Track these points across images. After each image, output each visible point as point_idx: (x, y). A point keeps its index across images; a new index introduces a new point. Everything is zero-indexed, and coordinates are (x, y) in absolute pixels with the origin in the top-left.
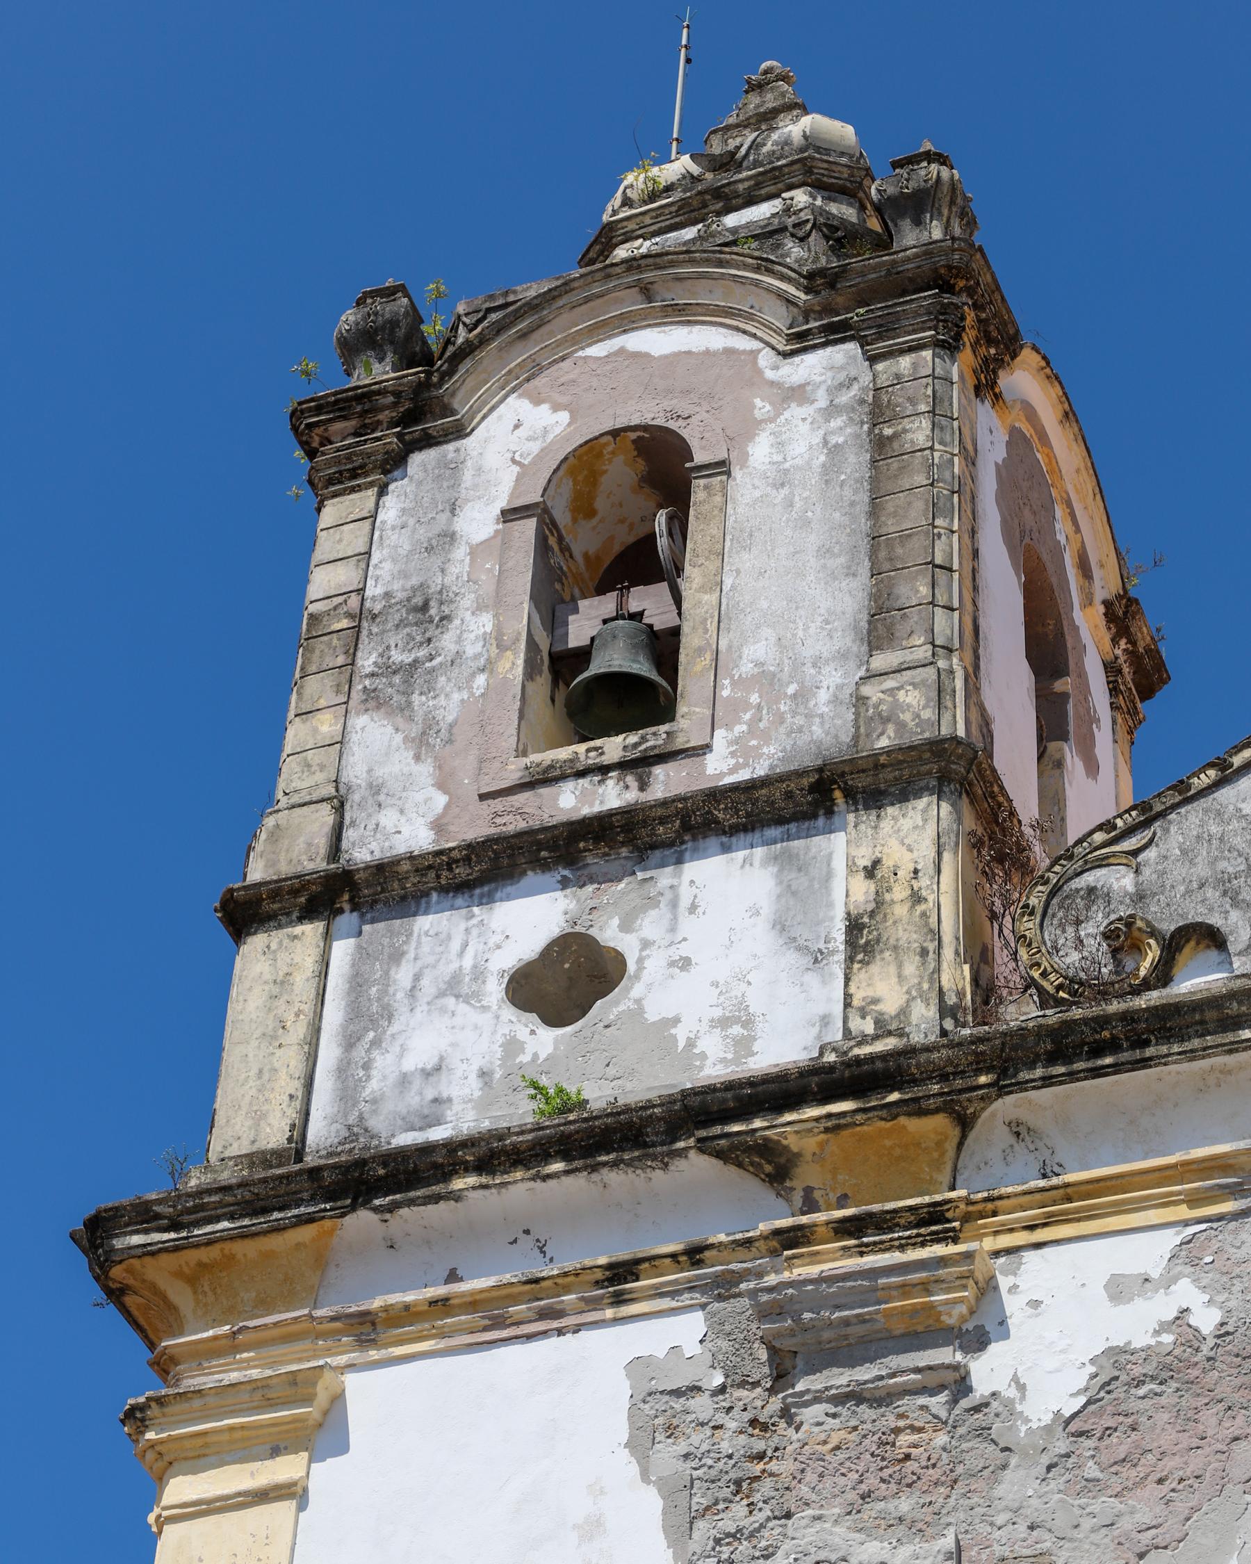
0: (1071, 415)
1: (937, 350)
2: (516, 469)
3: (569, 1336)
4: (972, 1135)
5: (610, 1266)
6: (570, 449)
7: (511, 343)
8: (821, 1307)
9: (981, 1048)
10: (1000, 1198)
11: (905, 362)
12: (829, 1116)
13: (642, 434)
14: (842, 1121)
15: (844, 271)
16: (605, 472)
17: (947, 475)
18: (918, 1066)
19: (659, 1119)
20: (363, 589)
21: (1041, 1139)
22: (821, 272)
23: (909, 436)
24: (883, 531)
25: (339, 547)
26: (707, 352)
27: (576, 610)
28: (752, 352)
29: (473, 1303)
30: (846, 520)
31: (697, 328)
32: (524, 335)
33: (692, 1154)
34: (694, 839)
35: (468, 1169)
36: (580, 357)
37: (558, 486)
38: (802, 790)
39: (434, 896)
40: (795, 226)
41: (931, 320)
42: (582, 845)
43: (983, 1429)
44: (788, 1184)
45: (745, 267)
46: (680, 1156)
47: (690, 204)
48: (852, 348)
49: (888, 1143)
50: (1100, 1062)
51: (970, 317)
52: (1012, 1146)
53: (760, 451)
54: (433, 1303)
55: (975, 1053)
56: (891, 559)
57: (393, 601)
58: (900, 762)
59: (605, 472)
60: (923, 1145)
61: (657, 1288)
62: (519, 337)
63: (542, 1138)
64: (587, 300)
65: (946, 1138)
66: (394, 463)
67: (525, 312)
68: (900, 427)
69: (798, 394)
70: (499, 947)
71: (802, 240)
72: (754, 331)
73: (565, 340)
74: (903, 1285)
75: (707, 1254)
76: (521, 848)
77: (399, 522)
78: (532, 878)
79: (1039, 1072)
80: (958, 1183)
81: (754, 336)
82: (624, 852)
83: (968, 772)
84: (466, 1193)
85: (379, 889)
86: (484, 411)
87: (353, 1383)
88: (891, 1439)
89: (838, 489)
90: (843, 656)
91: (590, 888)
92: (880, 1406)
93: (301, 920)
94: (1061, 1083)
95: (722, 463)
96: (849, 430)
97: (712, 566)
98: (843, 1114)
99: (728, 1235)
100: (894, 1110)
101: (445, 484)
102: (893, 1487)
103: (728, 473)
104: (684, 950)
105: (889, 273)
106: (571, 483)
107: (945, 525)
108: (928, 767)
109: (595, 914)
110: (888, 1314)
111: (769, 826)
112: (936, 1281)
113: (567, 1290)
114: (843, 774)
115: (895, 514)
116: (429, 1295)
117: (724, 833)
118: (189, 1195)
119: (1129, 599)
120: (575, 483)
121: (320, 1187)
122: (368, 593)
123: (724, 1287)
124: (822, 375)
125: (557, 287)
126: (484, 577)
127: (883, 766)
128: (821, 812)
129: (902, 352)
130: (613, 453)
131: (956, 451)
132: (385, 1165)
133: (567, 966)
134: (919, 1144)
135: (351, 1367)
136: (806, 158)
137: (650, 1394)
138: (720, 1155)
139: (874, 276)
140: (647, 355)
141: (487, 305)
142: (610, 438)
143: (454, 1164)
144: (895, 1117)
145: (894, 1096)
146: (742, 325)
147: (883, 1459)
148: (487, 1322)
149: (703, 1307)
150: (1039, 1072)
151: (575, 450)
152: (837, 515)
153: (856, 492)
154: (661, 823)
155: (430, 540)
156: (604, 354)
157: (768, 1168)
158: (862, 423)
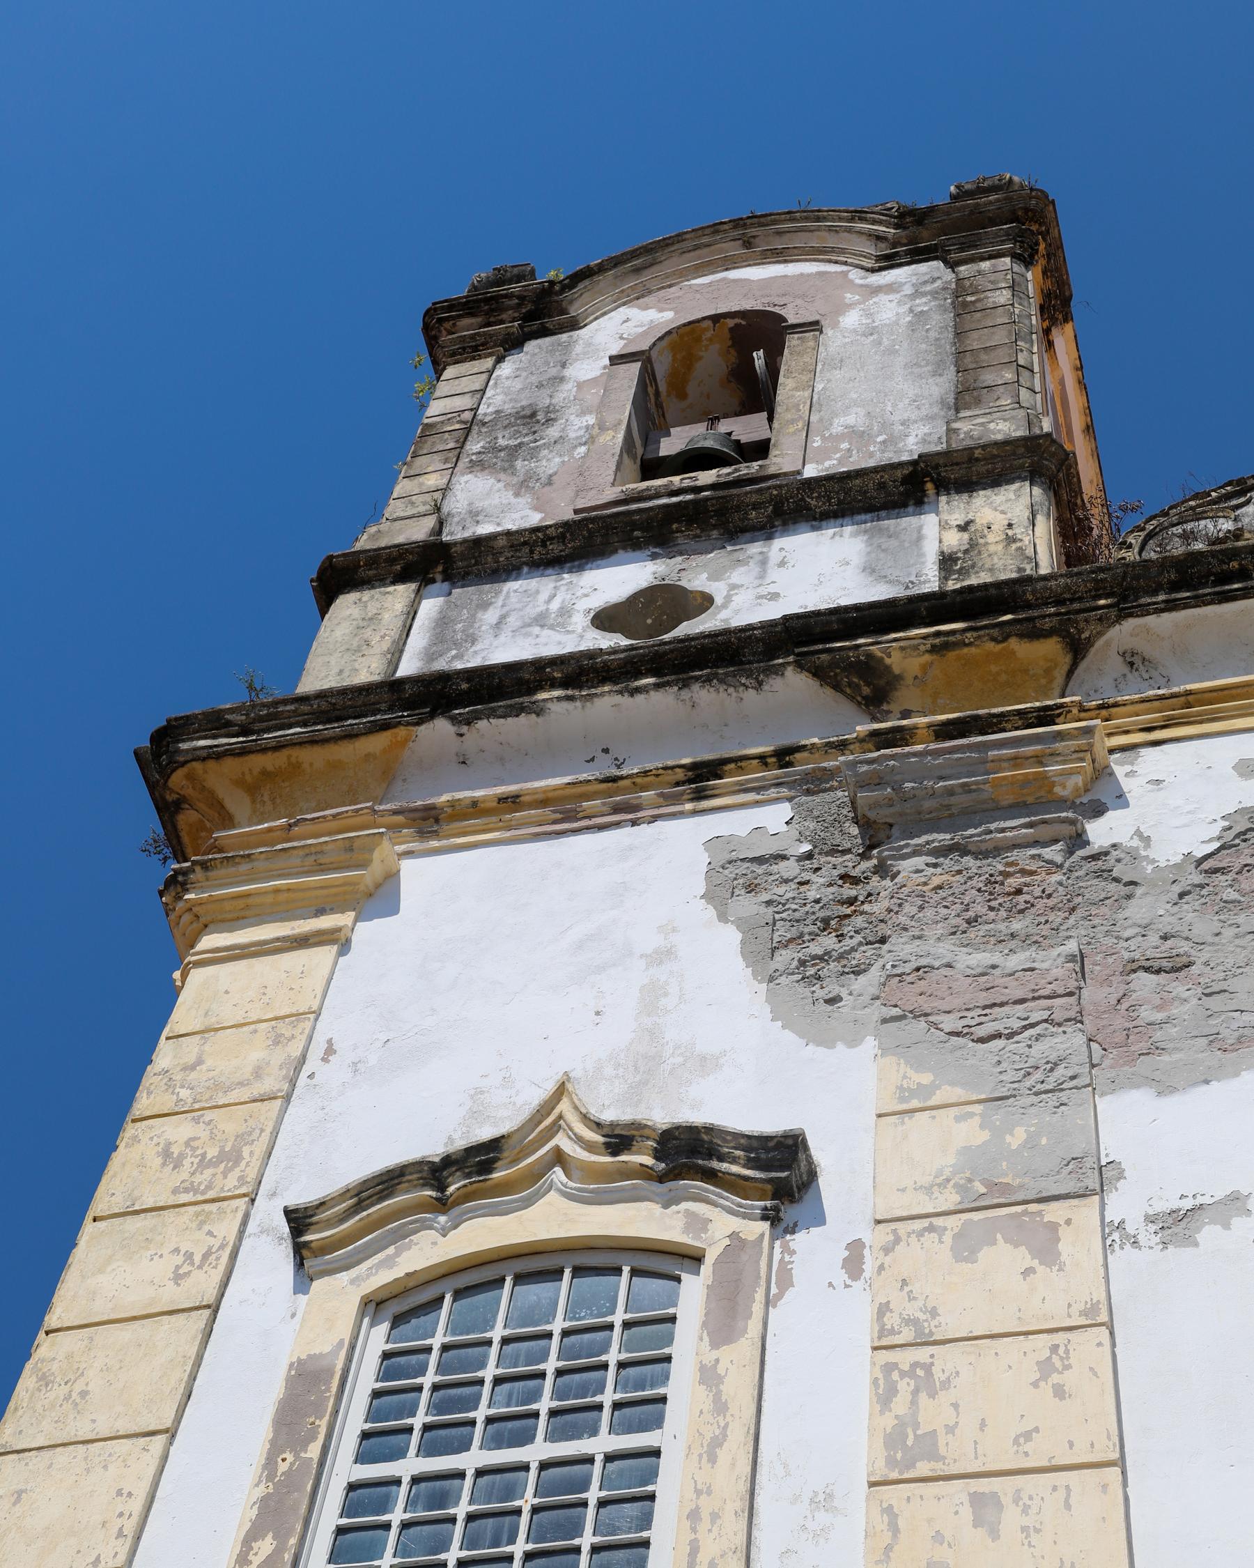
3: (644, 826)
4: (1083, 665)
5: (694, 766)
7: (625, 274)
8: (924, 778)
9: (1102, 576)
10: (1116, 705)
11: (985, 265)
12: (938, 634)
13: (737, 321)
14: (952, 639)
16: (701, 358)
18: (1034, 592)
19: (758, 640)
21: (1156, 669)
27: (668, 434)
29: (544, 801)
30: (933, 348)
32: (637, 270)
33: (789, 671)
34: (785, 524)
35: (554, 684)
38: (894, 481)
39: (525, 569)
42: (675, 526)
43: (1103, 871)
44: (885, 707)
46: (777, 674)
49: (994, 668)
50: (1227, 587)
51: (1042, 247)
52: (1124, 675)
53: (851, 319)
54: (502, 800)
55: (1095, 580)
56: (977, 362)
58: (995, 457)
59: (701, 358)
60: (1031, 672)
61: (743, 785)
63: (634, 657)
64: (696, 248)
65: (1056, 665)
67: (641, 254)
70: (586, 595)
74: (1016, 758)
75: (798, 756)
76: (616, 528)
78: (621, 554)
79: (1161, 597)
80: (1067, 692)
82: (715, 534)
83: (1058, 471)
84: (549, 705)
85: (473, 561)
87: (408, 868)
88: (1000, 878)
90: (930, 418)
91: (679, 559)
92: (986, 858)
93: (393, 583)
94: (1186, 607)
95: (817, 323)
96: (933, 303)
98: (953, 632)
99: (820, 739)
100: (1007, 629)
102: (1003, 913)
104: (772, 589)
105: (972, 213)
106: (670, 358)
108: (1021, 461)
109: (683, 574)
110: (997, 784)
111: (859, 513)
112: (1052, 755)
113: (644, 788)
114: (937, 466)
116: (498, 792)
117: (815, 519)
118: (264, 705)
120: (674, 360)
121: (399, 699)
123: (815, 783)
127: (977, 460)
128: (912, 502)
129: (983, 259)
130: (710, 340)
132: (468, 680)
133: (649, 621)
134: (1026, 671)
135: (409, 854)
137: (730, 862)
138: (818, 673)
142: (709, 323)
143: (541, 681)
145: (1009, 617)
147: (991, 894)
148: (559, 816)
149: (790, 799)
150: (1161, 597)
151: (678, 328)
154: (753, 509)
157: (866, 690)
158: (946, 299)
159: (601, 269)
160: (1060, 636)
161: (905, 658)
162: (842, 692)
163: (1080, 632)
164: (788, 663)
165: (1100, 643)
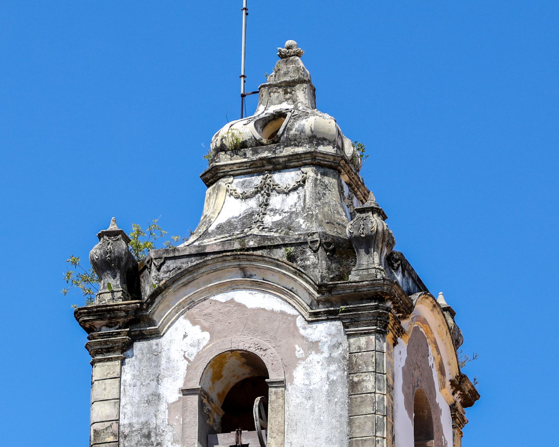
0: (436, 305)
1: (377, 335)
2: (187, 362)
6: (211, 358)
11: (363, 340)
15: (335, 287)
17: (382, 407)
20: (118, 420)
22: (326, 285)
23: (365, 384)
24: (354, 435)
25: (105, 393)
26: (272, 311)
28: (293, 316)
31: (267, 295)
32: (185, 285)
36: (213, 300)
37: (207, 373)
40: (311, 242)
41: (375, 320)
45: (289, 270)
47: (256, 164)
48: (338, 323)
57: (134, 429)
62: (183, 286)
66: (127, 346)
67: (186, 274)
68: (361, 378)
69: (314, 346)
71: (315, 252)
72: (294, 305)
73: (205, 290)
77: (132, 382)
81: (294, 307)
86: (169, 324)
89: (334, 406)
97: (280, 439)
101: (153, 364)
103: (285, 387)
105: (355, 291)
107: (380, 435)
115: (359, 427)
119: (461, 376)
122: (121, 422)
124: (326, 337)
125: (200, 263)
126: (175, 424)
130: (231, 356)
131: (385, 393)
136: (313, 152)
139: (348, 291)
140: (244, 306)
141: (165, 255)
146: (288, 300)
151: (213, 358)
152: (334, 421)
153: (342, 410)
155: (148, 396)
156: (224, 301)
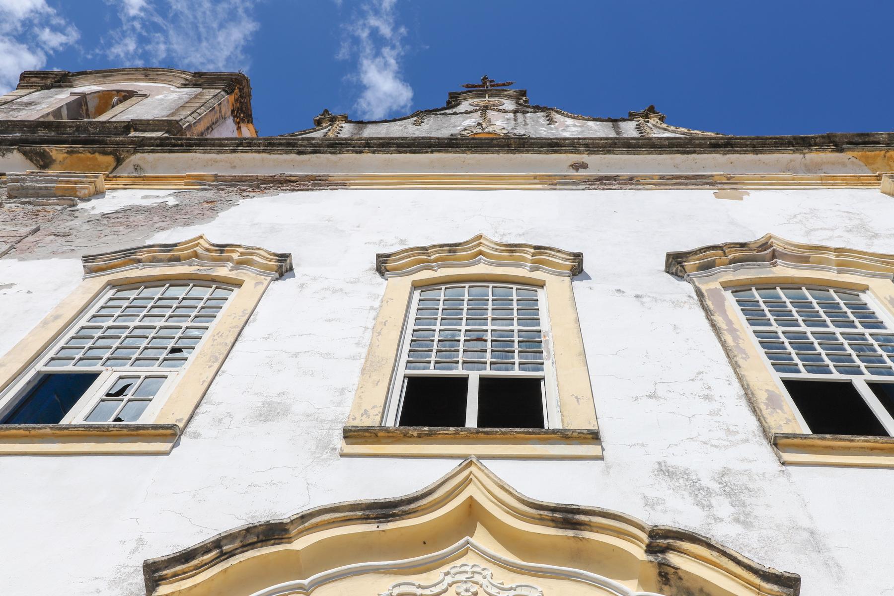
4: (120, 167)
10: (119, 177)
33: (15, 152)
49: (89, 163)
60: (101, 166)
65: (110, 165)
138: (25, 154)
144: (94, 153)
157: (42, 163)
159: (91, 73)
160: (113, 155)
161: (57, 154)
162: (33, 162)
163: (121, 155)
164: (15, 149)
165: (127, 160)
